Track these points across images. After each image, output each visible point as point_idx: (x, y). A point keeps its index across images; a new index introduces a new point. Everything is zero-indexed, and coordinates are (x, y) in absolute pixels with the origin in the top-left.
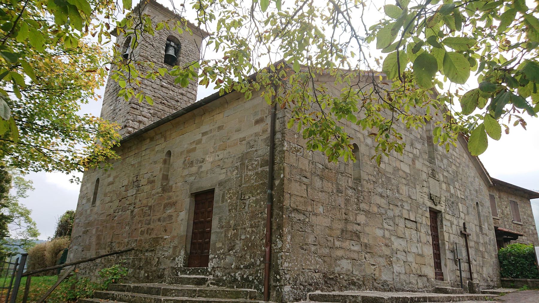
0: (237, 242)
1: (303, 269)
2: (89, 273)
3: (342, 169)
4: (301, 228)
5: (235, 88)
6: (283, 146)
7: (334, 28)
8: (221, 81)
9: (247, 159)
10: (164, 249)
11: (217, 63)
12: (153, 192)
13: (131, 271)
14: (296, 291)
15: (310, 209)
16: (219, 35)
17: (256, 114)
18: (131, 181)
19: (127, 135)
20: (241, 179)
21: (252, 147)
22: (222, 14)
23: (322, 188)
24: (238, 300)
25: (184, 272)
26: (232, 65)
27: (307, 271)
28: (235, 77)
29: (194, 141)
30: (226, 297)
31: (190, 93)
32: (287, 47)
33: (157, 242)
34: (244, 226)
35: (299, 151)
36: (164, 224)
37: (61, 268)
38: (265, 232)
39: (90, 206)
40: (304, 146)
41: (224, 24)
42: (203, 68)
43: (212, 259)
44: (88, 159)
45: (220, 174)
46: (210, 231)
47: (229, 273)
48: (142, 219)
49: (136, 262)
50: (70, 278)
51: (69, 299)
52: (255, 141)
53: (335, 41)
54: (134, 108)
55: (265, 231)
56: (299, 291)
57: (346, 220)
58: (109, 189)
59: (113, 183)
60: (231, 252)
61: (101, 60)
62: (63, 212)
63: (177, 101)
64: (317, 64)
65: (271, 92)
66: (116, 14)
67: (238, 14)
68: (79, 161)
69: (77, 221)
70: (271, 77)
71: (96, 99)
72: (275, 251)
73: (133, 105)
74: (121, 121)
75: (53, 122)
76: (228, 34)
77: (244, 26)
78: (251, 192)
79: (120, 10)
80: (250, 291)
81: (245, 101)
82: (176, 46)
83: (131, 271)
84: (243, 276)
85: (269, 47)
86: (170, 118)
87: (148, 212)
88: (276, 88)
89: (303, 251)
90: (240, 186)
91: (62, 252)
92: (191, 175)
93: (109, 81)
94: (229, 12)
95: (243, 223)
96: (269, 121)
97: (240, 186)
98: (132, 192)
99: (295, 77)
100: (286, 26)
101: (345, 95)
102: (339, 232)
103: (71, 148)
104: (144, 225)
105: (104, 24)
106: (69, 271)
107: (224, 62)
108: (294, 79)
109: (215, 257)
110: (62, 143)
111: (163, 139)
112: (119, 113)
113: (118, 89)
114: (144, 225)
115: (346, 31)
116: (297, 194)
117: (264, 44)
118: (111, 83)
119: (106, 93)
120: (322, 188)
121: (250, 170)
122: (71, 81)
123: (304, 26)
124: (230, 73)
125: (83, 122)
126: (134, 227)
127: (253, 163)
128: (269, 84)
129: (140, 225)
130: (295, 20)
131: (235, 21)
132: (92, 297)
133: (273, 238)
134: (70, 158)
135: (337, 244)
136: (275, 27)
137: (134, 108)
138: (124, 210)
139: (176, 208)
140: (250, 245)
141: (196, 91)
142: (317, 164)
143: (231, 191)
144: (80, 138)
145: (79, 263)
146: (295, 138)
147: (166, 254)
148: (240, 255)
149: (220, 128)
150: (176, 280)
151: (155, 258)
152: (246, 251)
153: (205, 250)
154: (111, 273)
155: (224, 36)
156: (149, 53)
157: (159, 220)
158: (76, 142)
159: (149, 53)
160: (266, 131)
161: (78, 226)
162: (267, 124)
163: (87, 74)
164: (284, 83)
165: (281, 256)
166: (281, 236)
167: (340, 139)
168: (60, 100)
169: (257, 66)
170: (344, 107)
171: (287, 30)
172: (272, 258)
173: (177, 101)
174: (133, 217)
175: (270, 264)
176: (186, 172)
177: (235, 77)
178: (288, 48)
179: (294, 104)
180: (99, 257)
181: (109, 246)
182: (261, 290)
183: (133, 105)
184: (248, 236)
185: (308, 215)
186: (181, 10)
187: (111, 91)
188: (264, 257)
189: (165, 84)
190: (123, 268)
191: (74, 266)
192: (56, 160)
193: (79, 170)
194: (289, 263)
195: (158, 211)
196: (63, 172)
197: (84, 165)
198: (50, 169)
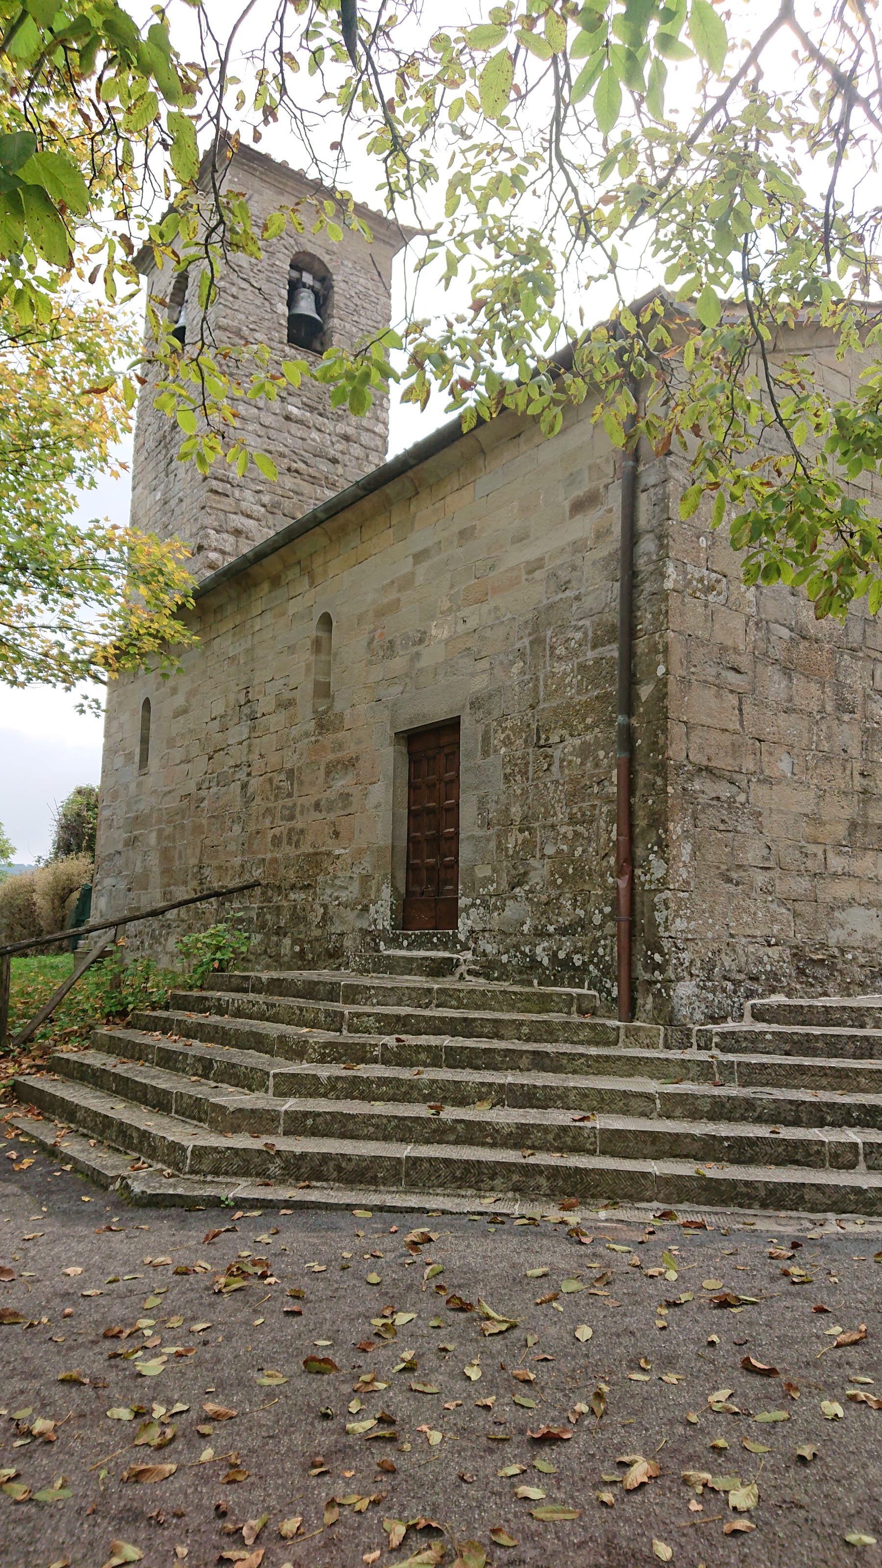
0: (533, 862)
1: (732, 936)
2: (151, 946)
3: (856, 635)
4: (723, 821)
5: (508, 402)
6: (663, 576)
7: (837, 160)
8: (467, 385)
9: (549, 624)
10: (338, 882)
11: (450, 325)
12: (295, 732)
13: (256, 939)
14: (710, 996)
15: (749, 764)
16: (457, 231)
17: (572, 480)
18: (232, 704)
19: (209, 573)
20: (536, 686)
21: (565, 586)
22: (459, 160)
23: (790, 700)
24: (544, 1017)
25: (394, 942)
26: (499, 327)
27: (744, 941)
28: (509, 364)
29: (393, 582)
30: (512, 1007)
31: (368, 430)
32: (674, 244)
33: (318, 865)
34: (550, 820)
35: (714, 589)
36: (332, 817)
37: (77, 937)
38: (614, 836)
39: (136, 773)
40: (728, 573)
41: (465, 191)
42: (411, 348)
43: (467, 909)
44: (116, 648)
45: (473, 675)
46: (457, 834)
47: (516, 947)
48: (270, 805)
49: (268, 917)
50: (107, 961)
51: (108, 1014)
52: (574, 568)
53: (838, 205)
54: (216, 492)
55: (615, 832)
56: (720, 996)
57: (865, 792)
58: (177, 727)
59: (185, 711)
60: (517, 890)
61: (115, 354)
62: (66, 793)
63: (334, 461)
64: (777, 291)
65: (625, 404)
66: (146, 204)
67: (509, 150)
68: (93, 655)
69: (106, 813)
70: (621, 351)
71: (116, 475)
72: (647, 887)
73: (214, 482)
74: (188, 532)
75: (10, 547)
76: (485, 222)
77: (530, 190)
78: (566, 724)
79: (157, 188)
80: (579, 995)
81: (537, 440)
82: (318, 285)
83: (256, 939)
84: (555, 954)
85: (614, 250)
86: (321, 516)
87: (286, 785)
88: (637, 385)
89: (730, 888)
90: (532, 707)
91: (76, 895)
92: (392, 681)
93: (140, 415)
94: (479, 148)
95: (547, 812)
96: (615, 499)
97: (532, 707)
98: (238, 732)
99: (701, 345)
100: (672, 171)
101: (872, 388)
102: (841, 830)
103: (66, 618)
104: (278, 821)
105: (116, 239)
106: (101, 944)
107: (474, 320)
108: (697, 351)
109: (473, 905)
110: (43, 606)
111: (306, 580)
112: (178, 511)
113: (168, 438)
114: (278, 821)
115: (876, 170)
116: (708, 721)
117: (598, 242)
118: (147, 420)
119: (137, 451)
120: (790, 700)
121: (560, 659)
122: (41, 422)
123: (732, 165)
124: (493, 354)
125: (90, 543)
126: (252, 827)
127: (570, 635)
128: (614, 379)
129: (268, 821)
130: (702, 149)
131: (500, 176)
132: (166, 1008)
133: (640, 852)
134: (69, 647)
135: (836, 863)
136: (633, 179)
137: (216, 492)
138: (223, 781)
139: (358, 775)
140: (571, 871)
141: (385, 424)
142: (772, 626)
143: (509, 724)
144: (86, 589)
145: (125, 921)
146: (699, 549)
147: (344, 896)
148: (544, 898)
149: (465, 535)
150: (375, 963)
151: (316, 906)
152: (559, 887)
153: (446, 883)
154: (208, 946)
155: (474, 232)
156: (243, 317)
157: (317, 806)
158: (78, 600)
159: (243, 317)
160: (609, 532)
161: (110, 827)
162: (610, 510)
163: (83, 400)
164: (665, 369)
165: (666, 902)
166: (663, 845)
167: (856, 542)
168: (21, 484)
169: (573, 322)
170: (871, 431)
171: (675, 187)
172: (638, 905)
173: (334, 461)
174: (248, 800)
175: (632, 924)
176: (376, 674)
177: (509, 364)
178: (680, 246)
179: (697, 435)
180: (173, 907)
181: (194, 876)
182: (609, 993)
183: (214, 484)
184: (565, 847)
185: (744, 785)
186: (335, 165)
187: (150, 444)
188: (615, 904)
189: (295, 411)
190: (237, 933)
191: (113, 931)
192: (31, 654)
193: (95, 678)
194: (689, 919)
195: (312, 784)
196: (54, 686)
197: (107, 663)
198: (22, 678)
